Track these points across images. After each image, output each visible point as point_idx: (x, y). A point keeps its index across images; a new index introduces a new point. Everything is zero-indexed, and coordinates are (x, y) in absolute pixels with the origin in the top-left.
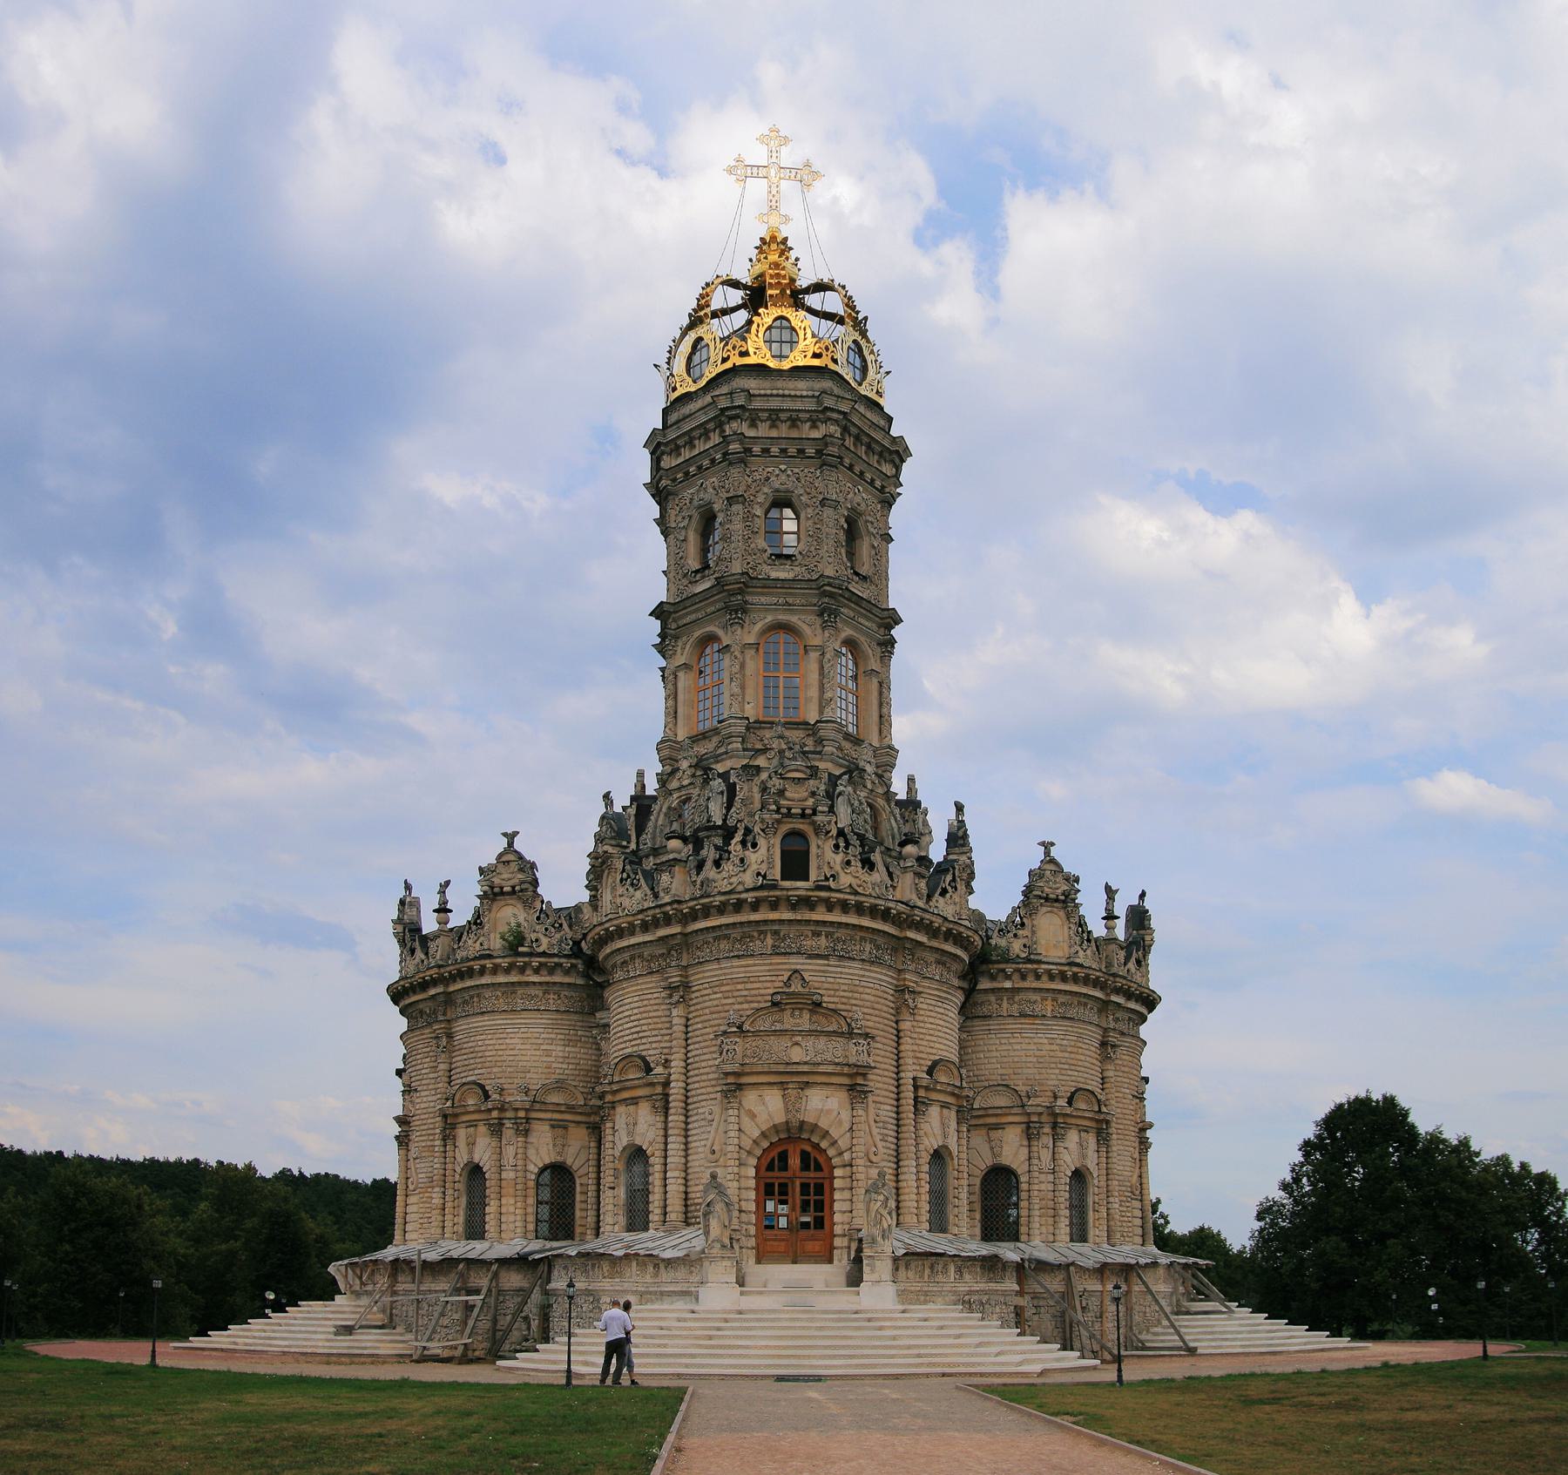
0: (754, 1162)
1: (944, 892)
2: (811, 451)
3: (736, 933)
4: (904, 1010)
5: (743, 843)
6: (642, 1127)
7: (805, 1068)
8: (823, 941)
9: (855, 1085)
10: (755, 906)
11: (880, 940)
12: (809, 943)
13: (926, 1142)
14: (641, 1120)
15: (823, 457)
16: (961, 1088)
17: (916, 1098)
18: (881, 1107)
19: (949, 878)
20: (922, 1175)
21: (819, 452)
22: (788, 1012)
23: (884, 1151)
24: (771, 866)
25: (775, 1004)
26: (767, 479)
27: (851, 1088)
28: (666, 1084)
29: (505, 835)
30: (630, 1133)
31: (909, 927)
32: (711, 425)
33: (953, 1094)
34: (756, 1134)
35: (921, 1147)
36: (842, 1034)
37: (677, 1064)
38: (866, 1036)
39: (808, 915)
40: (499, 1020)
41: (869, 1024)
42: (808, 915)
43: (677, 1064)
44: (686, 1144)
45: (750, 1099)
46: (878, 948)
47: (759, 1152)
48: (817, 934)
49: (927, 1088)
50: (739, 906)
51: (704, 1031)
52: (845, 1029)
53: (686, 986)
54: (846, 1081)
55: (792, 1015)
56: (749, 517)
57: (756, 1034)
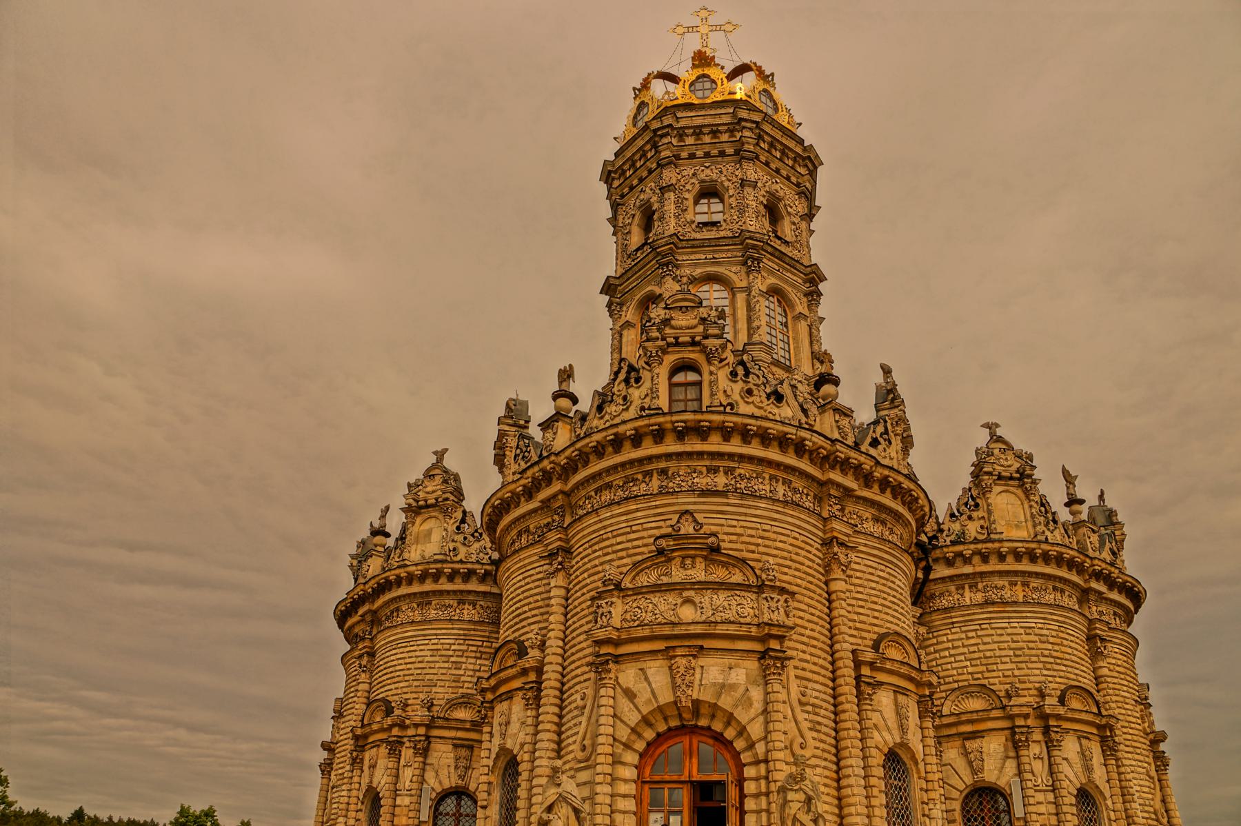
0: (631, 758)
2: (730, 151)
3: (617, 479)
4: (835, 567)
5: (627, 381)
6: (514, 727)
7: (698, 629)
9: (769, 650)
10: (637, 440)
11: (798, 483)
12: (703, 481)
13: (877, 738)
14: (514, 718)
15: (740, 155)
16: (920, 670)
17: (858, 678)
18: (804, 681)
19: (880, 429)
20: (873, 781)
21: (737, 152)
22: (678, 561)
23: (815, 747)
24: (653, 393)
25: (661, 552)
26: (695, 174)
27: (763, 655)
28: (539, 671)
29: (435, 453)
30: (503, 735)
31: (833, 468)
32: (648, 147)
33: (911, 679)
35: (869, 743)
36: (745, 587)
37: (554, 644)
38: (782, 591)
39: (696, 446)
40: (410, 631)
41: (786, 578)
42: (696, 446)
43: (554, 644)
44: (559, 743)
45: (628, 675)
46: (795, 491)
47: (640, 746)
48: (713, 470)
49: (871, 665)
50: (617, 443)
51: (581, 601)
52: (753, 580)
53: (568, 551)
54: (758, 647)
55: (683, 566)
56: (679, 202)
57: (638, 591)
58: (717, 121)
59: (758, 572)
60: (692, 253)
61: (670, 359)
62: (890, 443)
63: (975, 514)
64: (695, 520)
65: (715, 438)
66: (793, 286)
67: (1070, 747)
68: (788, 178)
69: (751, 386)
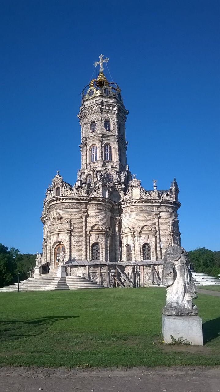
0: (54, 249)
1: (95, 191)
2: (96, 111)
7: (58, 231)
8: (63, 206)
11: (76, 204)
34: (52, 244)
47: (54, 247)
48: (62, 205)
58: (93, 104)
59: (67, 220)
60: (89, 140)
61: (56, 187)
62: (99, 190)
63: (129, 194)
64: (59, 214)
65: (61, 200)
66: (112, 141)
67: (143, 237)
68: (111, 112)
69: (68, 190)
